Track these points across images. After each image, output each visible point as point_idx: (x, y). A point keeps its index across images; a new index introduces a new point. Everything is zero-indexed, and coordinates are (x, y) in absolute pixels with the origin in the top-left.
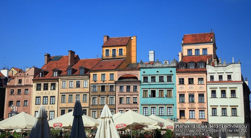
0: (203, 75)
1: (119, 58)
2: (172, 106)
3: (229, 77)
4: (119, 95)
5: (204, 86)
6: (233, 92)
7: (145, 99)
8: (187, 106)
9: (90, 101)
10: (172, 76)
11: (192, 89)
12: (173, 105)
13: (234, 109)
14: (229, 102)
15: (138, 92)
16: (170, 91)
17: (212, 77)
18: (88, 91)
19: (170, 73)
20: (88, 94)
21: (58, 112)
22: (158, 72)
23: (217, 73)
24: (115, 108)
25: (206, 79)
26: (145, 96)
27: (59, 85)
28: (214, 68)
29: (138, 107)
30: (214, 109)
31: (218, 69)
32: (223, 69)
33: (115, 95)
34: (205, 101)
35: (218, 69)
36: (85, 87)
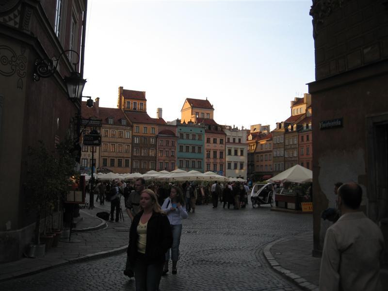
0: (223, 137)
1: (141, 112)
3: (240, 140)
4: (159, 148)
5: (224, 146)
6: (242, 152)
7: (181, 153)
8: (212, 161)
12: (202, 159)
16: (200, 148)
17: (229, 139)
19: (201, 133)
22: (191, 130)
26: (181, 150)
30: (229, 164)
34: (224, 157)
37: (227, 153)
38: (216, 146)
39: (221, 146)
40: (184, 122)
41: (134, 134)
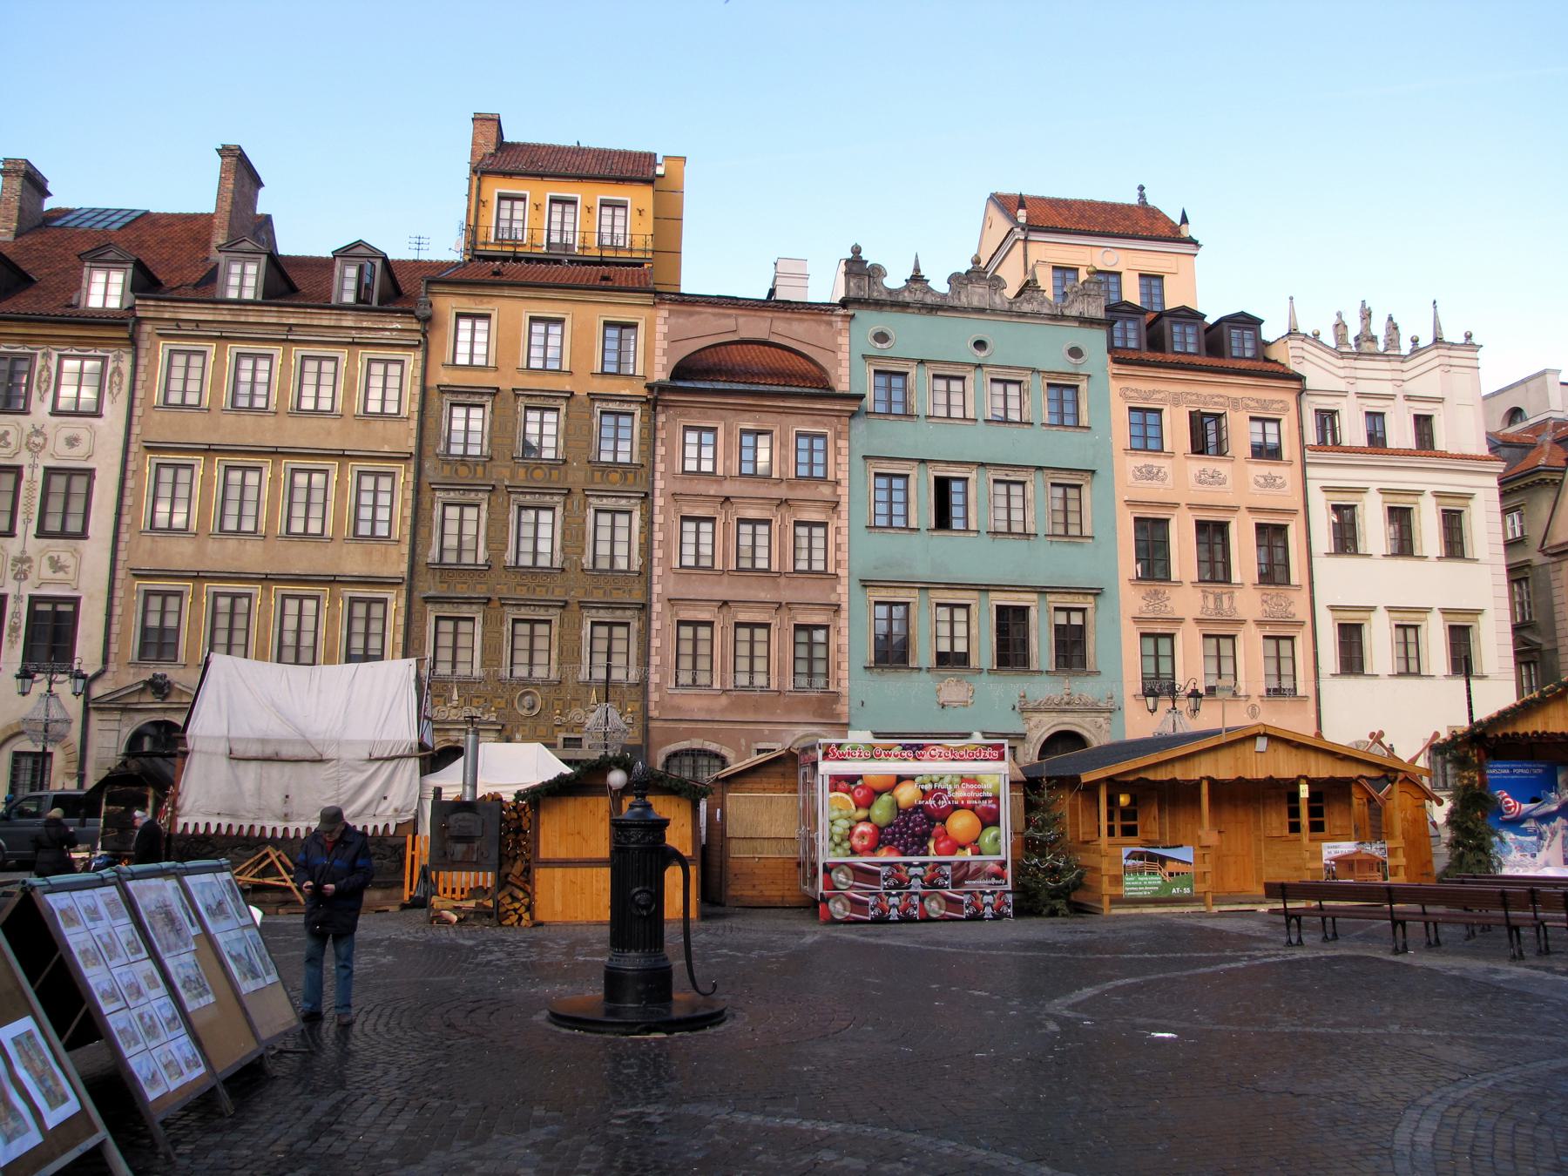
0: (1277, 397)
2: (1087, 602)
5: (1286, 473)
6: (1452, 523)
7: (893, 545)
8: (1186, 598)
9: (423, 531)
10: (1083, 385)
11: (1216, 487)
12: (1097, 593)
13: (1460, 639)
14: (1432, 584)
15: (837, 483)
17: (1327, 418)
18: (411, 445)
19: (1063, 363)
20: (404, 475)
21: (118, 611)
22: (980, 344)
23: (1361, 395)
24: (637, 597)
25: (1301, 427)
27: (142, 376)
28: (1341, 363)
29: (833, 599)
30: (1351, 636)
31: (1360, 374)
32: (1389, 375)
33: (647, 498)
34: (1297, 573)
35: (1360, 374)
36: (374, 407)
37: (1323, 539)
38: (1216, 479)
39: (1270, 482)
40: (917, 278)
41: (443, 377)
